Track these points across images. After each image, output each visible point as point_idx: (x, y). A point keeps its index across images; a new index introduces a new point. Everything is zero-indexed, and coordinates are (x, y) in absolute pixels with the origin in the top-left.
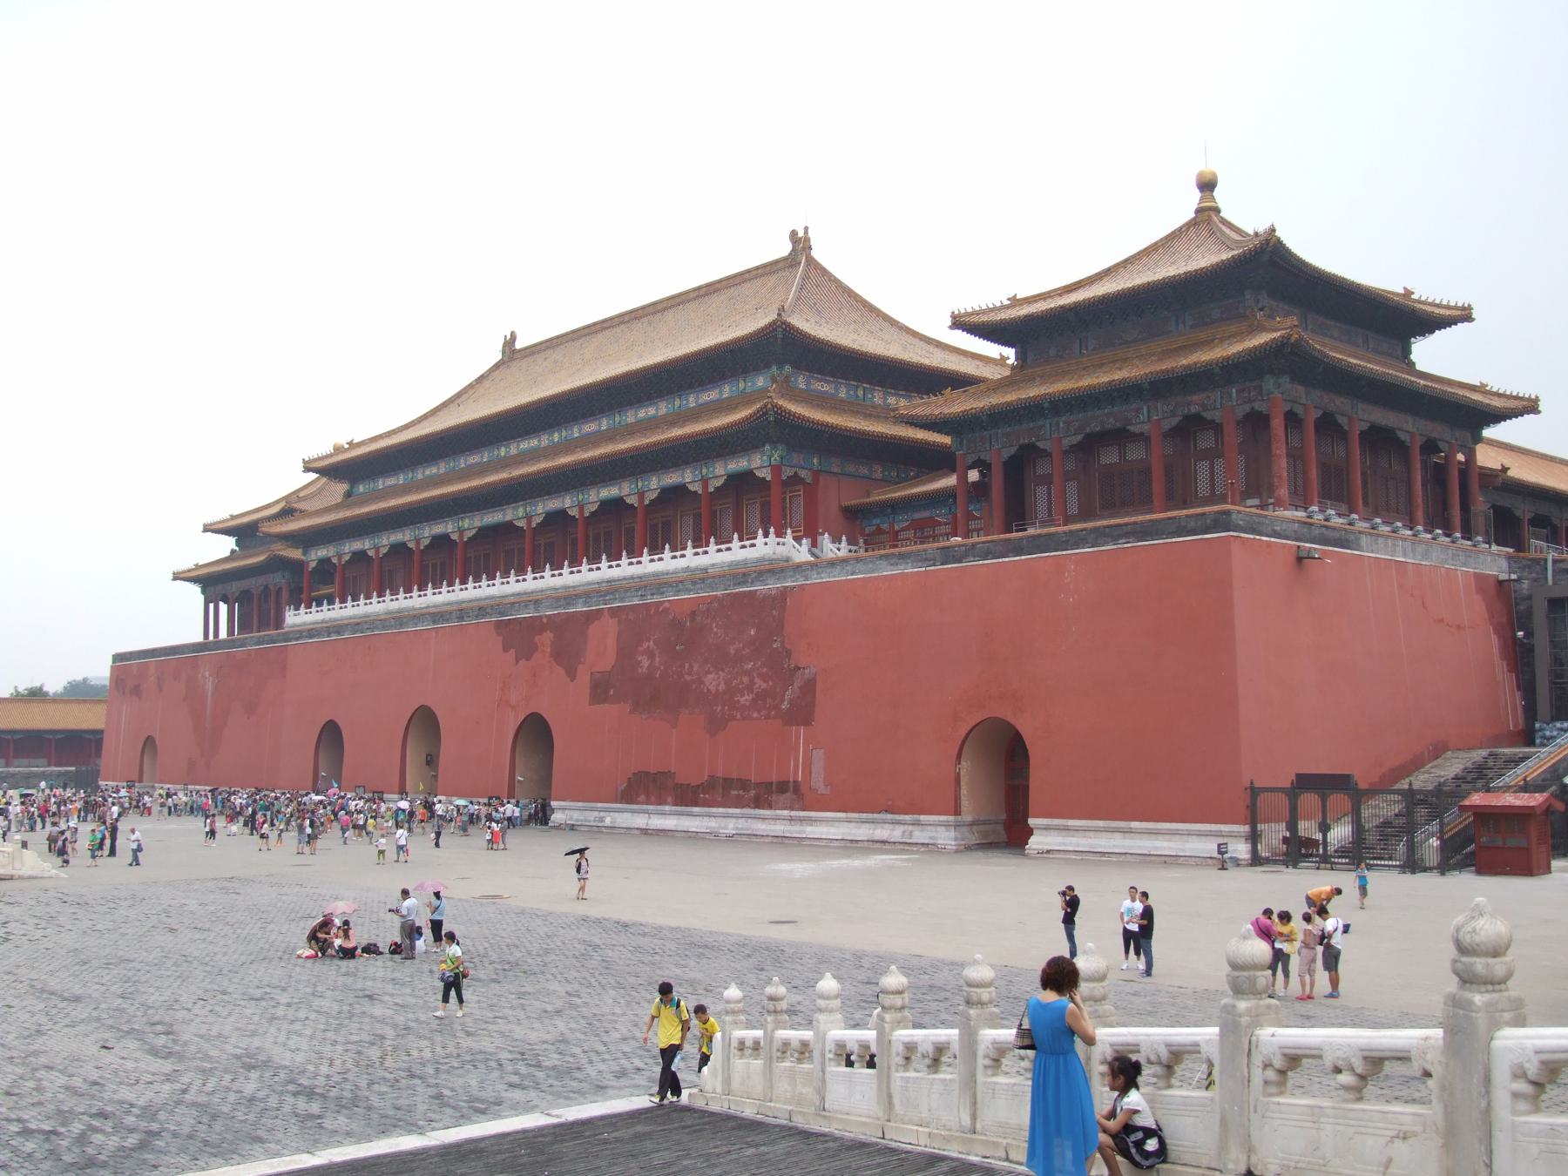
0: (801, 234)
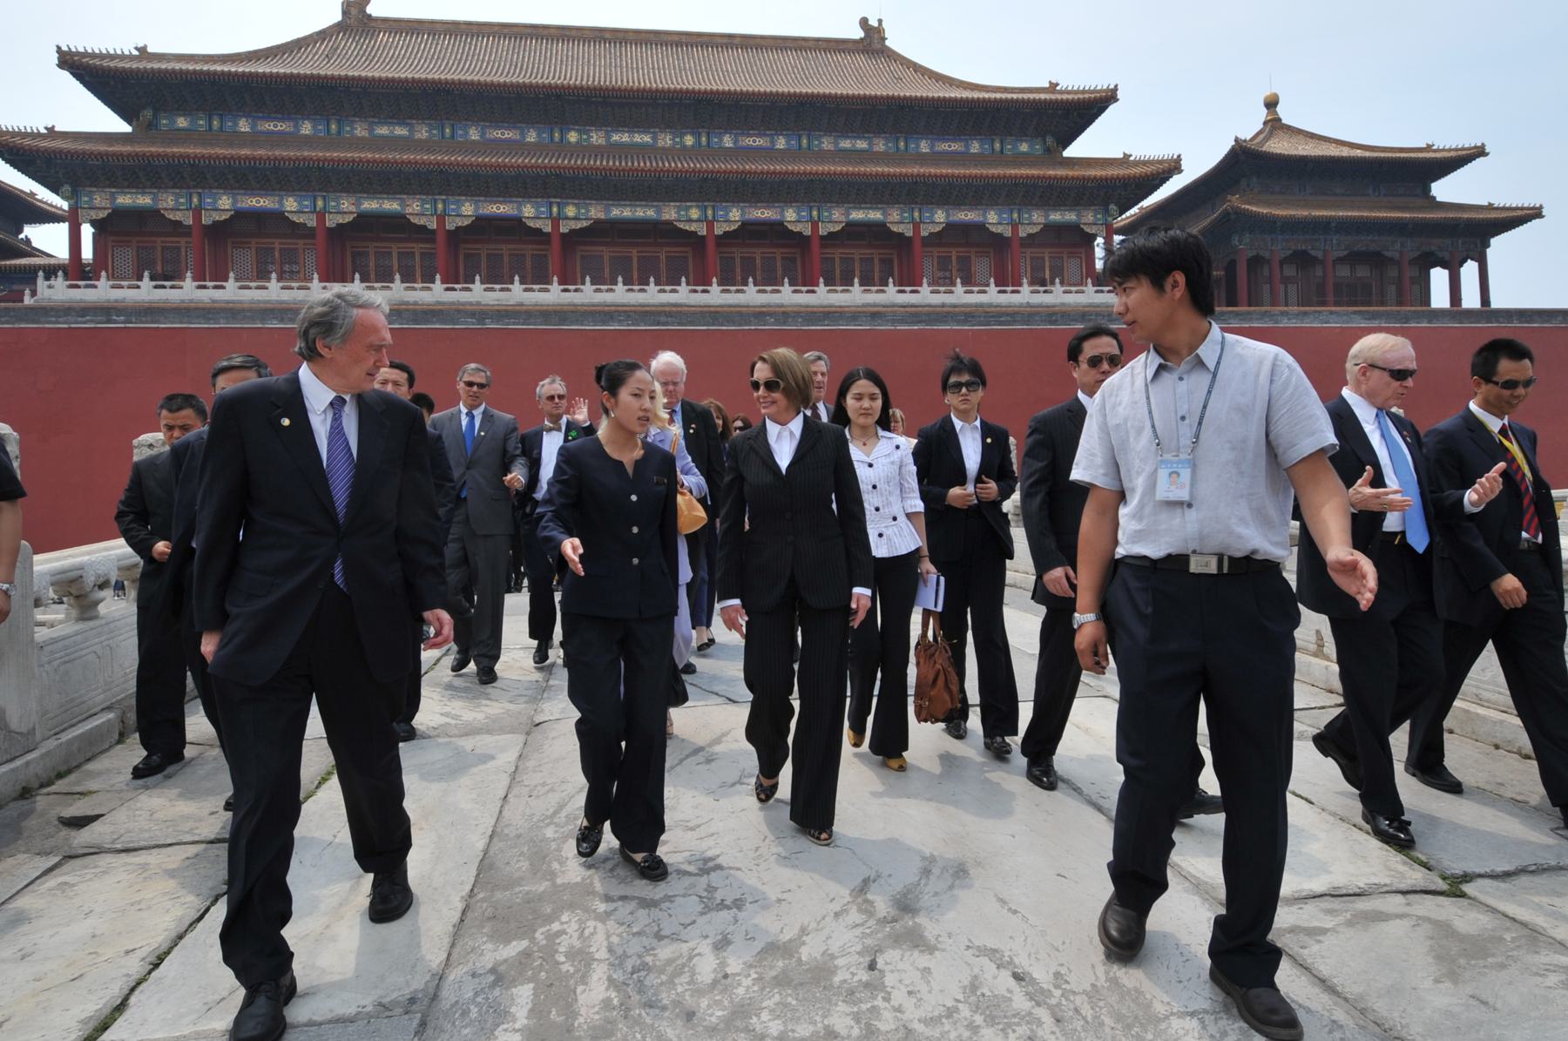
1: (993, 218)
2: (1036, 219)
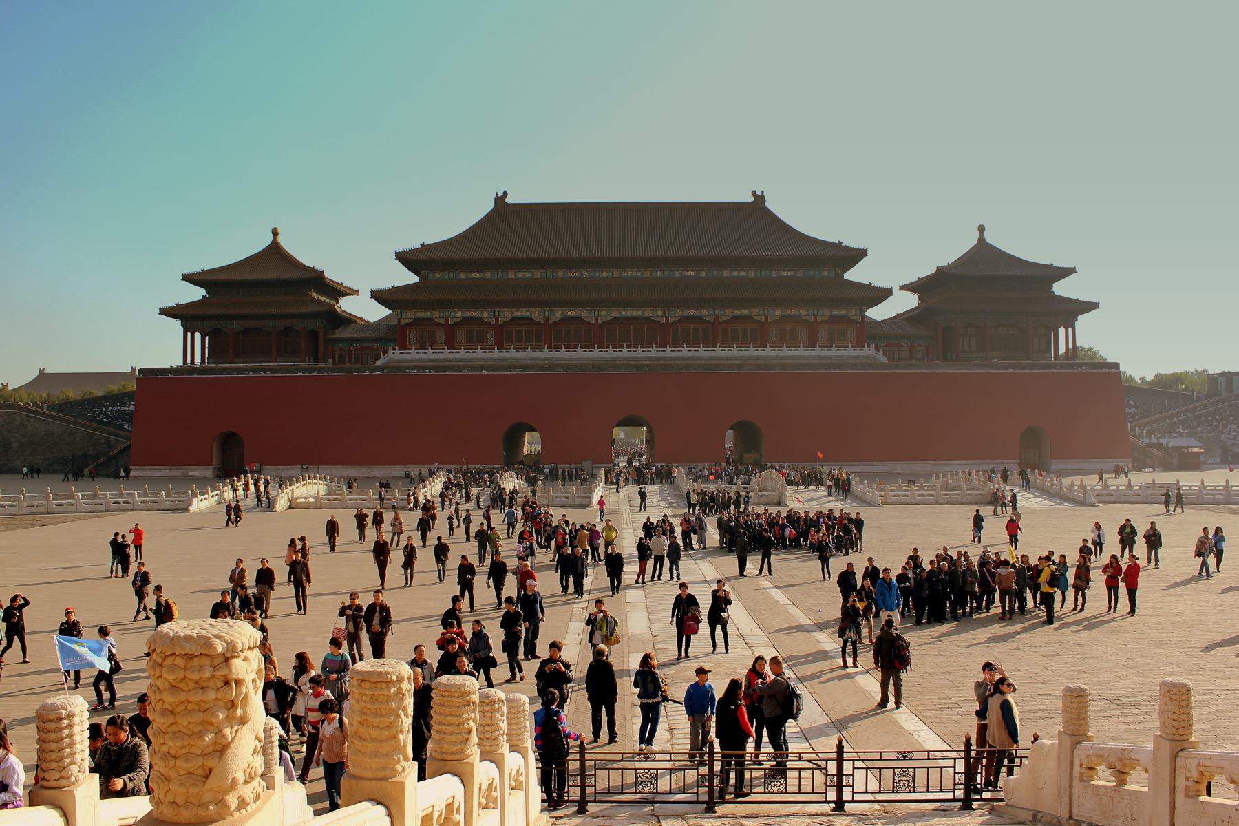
0: (759, 193)
2: (826, 312)
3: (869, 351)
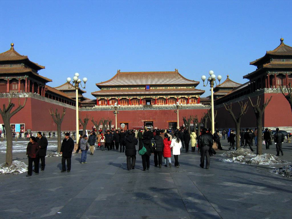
0: (177, 69)
1: (186, 96)
3: (200, 104)
